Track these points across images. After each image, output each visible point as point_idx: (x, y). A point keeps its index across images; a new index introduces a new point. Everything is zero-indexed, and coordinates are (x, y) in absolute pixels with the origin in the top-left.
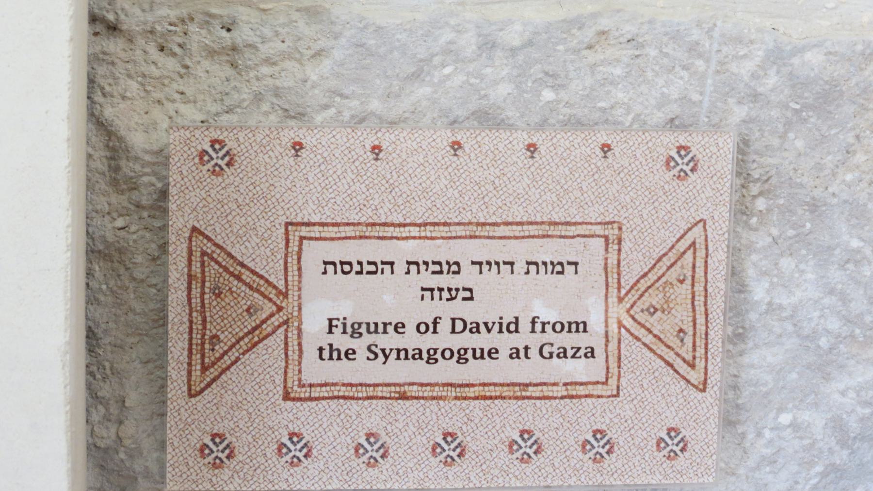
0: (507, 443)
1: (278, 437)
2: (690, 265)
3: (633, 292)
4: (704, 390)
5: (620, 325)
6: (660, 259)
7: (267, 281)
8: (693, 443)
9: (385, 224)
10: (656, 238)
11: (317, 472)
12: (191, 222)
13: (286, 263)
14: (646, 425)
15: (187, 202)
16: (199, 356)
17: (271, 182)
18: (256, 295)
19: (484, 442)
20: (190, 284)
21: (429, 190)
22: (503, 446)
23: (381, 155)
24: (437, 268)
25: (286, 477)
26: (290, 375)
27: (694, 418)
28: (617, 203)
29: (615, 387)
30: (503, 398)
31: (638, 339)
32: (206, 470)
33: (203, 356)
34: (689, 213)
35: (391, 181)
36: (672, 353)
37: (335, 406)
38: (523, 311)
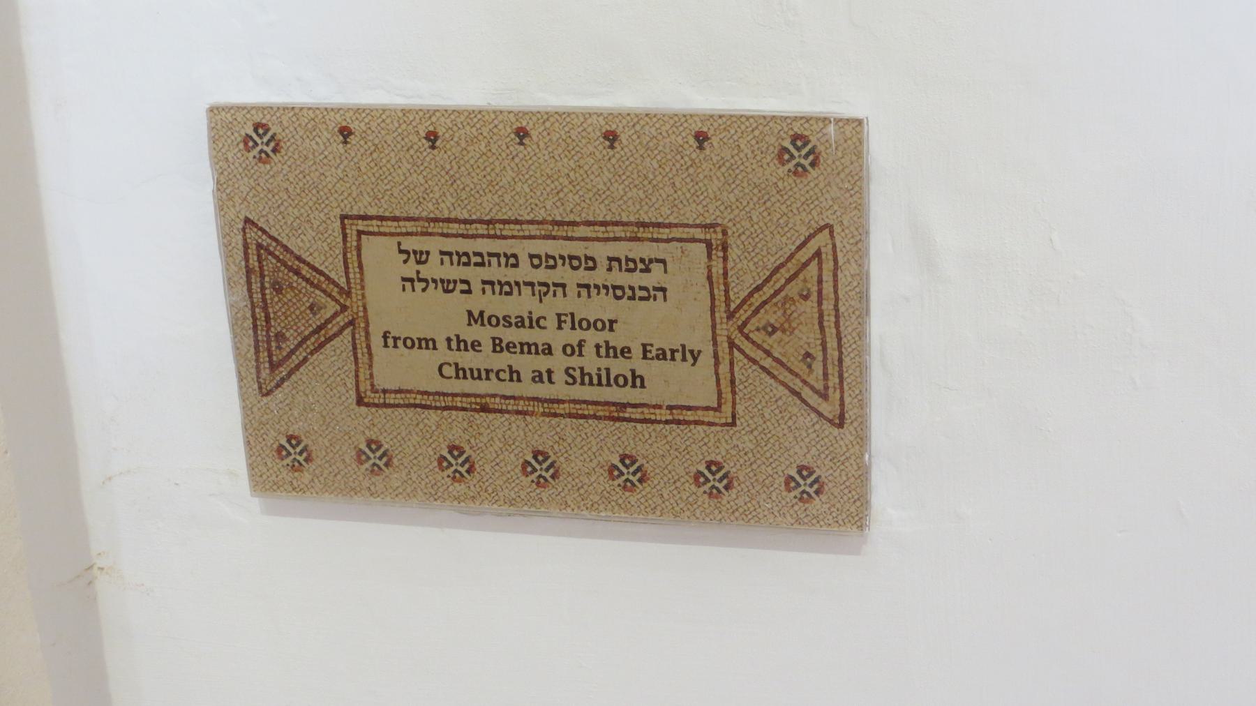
0: (606, 468)
1: (356, 443)
2: (815, 279)
3: (745, 307)
5: (732, 345)
6: (777, 270)
8: (830, 485)
9: (448, 220)
11: (400, 484)
12: (243, 212)
14: (771, 460)
16: (266, 354)
17: (322, 171)
18: (317, 292)
19: (580, 464)
20: (248, 278)
21: (494, 183)
22: (601, 471)
23: (438, 143)
25: (368, 485)
26: (362, 377)
27: (830, 457)
28: (720, 202)
29: (729, 415)
31: (754, 361)
32: (286, 472)
34: (810, 217)
35: (452, 173)
36: (798, 381)
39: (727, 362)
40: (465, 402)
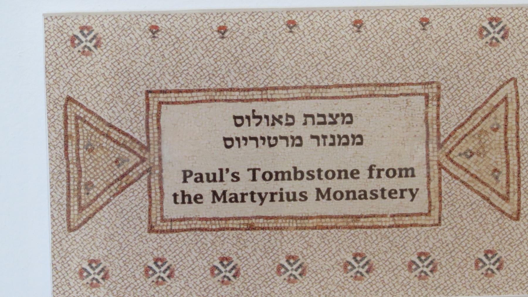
0: (342, 264)
1: (145, 262)
2: (503, 116)
3: (451, 139)
4: (517, 219)
5: (440, 166)
7: (132, 138)
8: (508, 262)
9: (231, 90)
10: (471, 94)
11: (179, 289)
12: (65, 93)
13: (147, 123)
14: (466, 248)
15: (62, 77)
16: (76, 199)
17: (133, 59)
18: (123, 149)
19: (322, 263)
20: (66, 142)
22: (339, 267)
23: (226, 34)
25: (153, 293)
26: (154, 211)
27: (508, 242)
28: (436, 67)
29: (437, 217)
30: (337, 228)
31: (456, 178)
32: (85, 289)
33: (79, 199)
34: (500, 73)
35: (236, 55)
36: (487, 189)
37: (192, 236)
38: (354, 157)
39: (437, 179)
40: (235, 224)
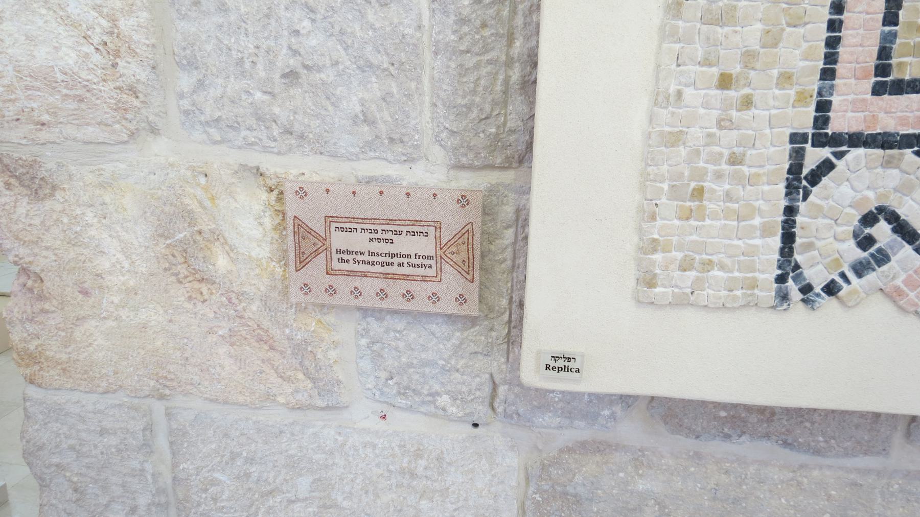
5: (441, 257)
6: (455, 235)
9: (358, 218)
24: (370, 231)
33: (300, 258)
